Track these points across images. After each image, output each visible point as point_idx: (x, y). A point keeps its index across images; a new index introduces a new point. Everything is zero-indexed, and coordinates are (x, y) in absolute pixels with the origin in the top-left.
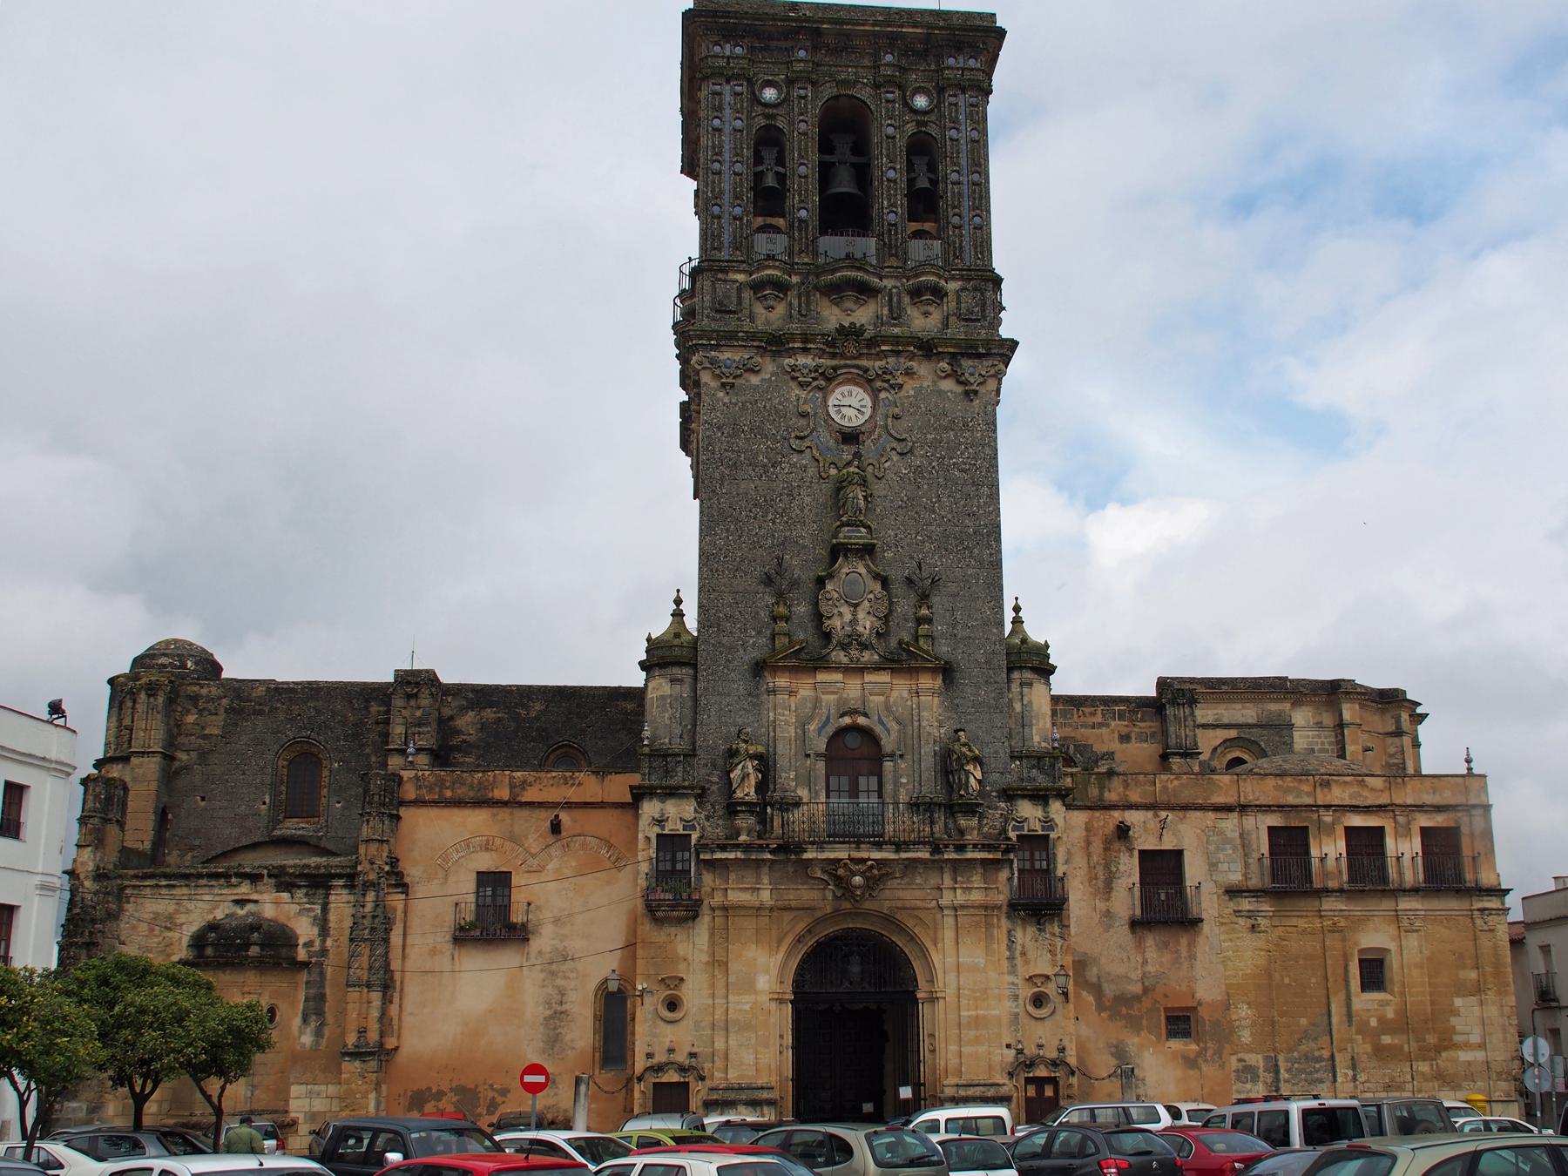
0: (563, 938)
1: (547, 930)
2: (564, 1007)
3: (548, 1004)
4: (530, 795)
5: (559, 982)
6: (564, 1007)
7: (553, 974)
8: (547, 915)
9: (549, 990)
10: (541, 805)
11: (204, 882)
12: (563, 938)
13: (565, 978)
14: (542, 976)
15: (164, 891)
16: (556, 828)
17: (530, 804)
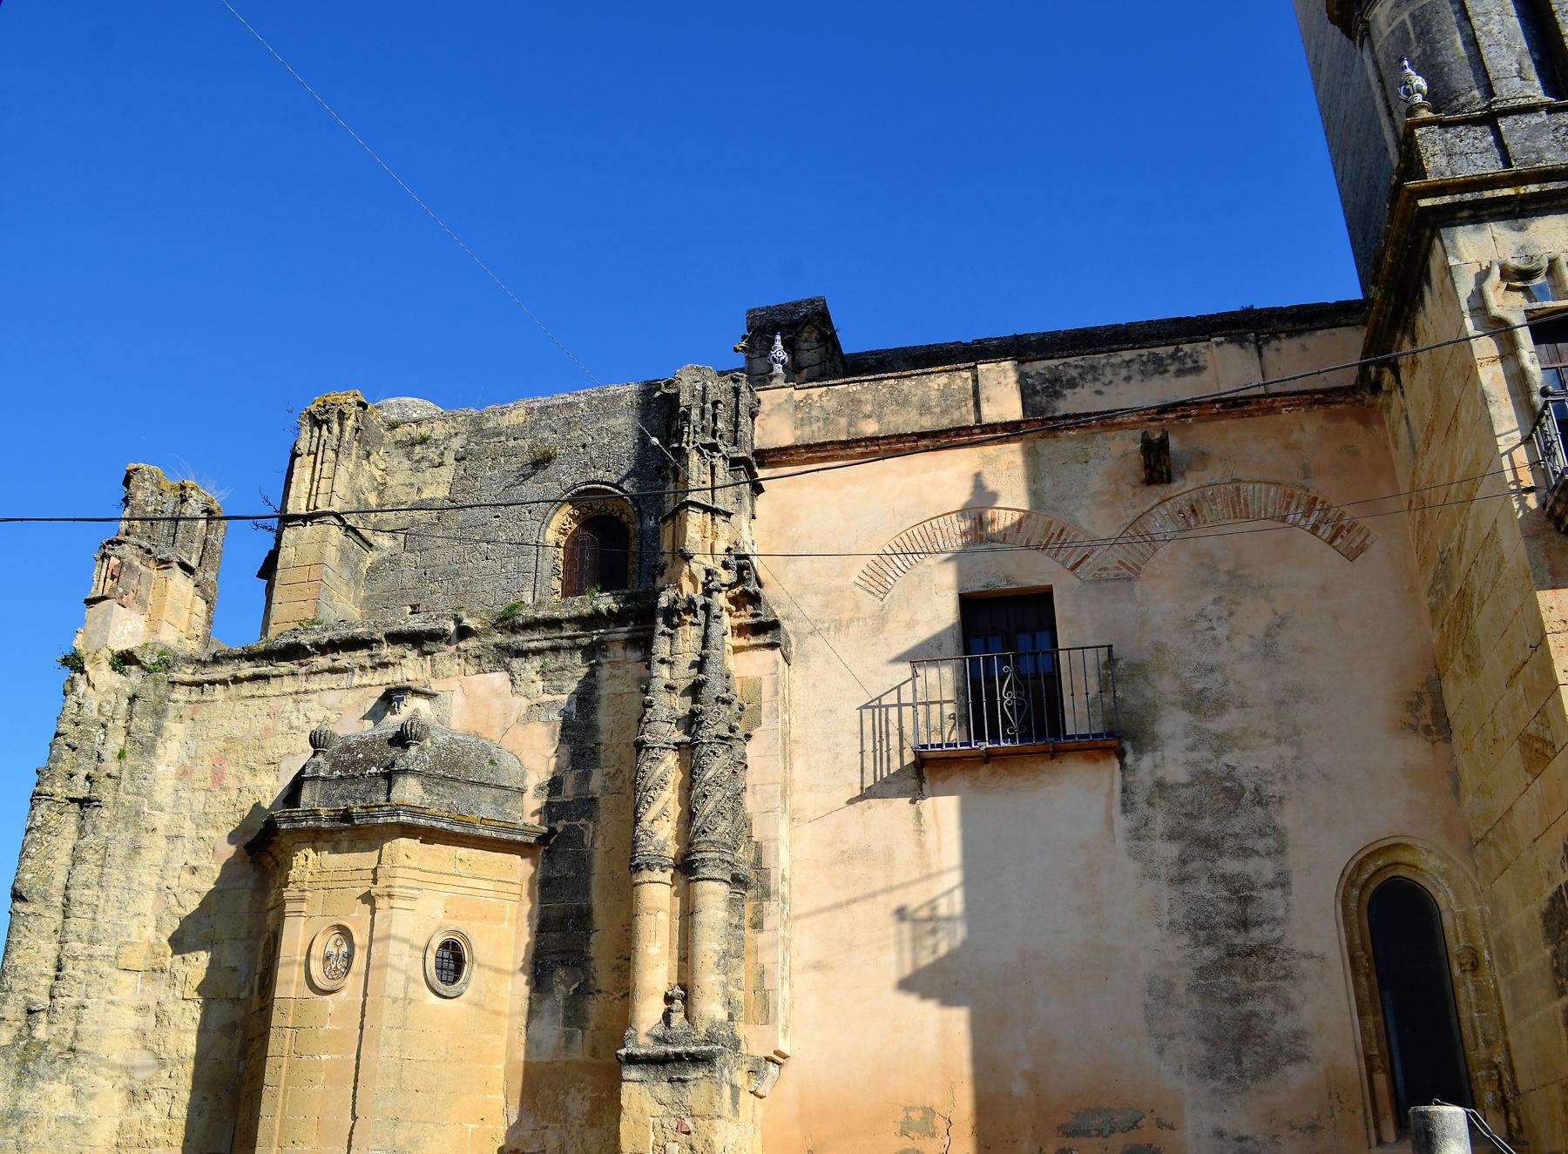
0: (1223, 743)
1: (1172, 724)
2: (1257, 935)
3: (1201, 928)
4: (1075, 401)
5: (1230, 866)
6: (1257, 935)
7: (1209, 844)
8: (1166, 686)
9: (1203, 888)
10: (1107, 420)
11: (322, 662)
12: (1223, 743)
13: (1247, 853)
14: (1173, 850)
15: (247, 688)
16: (1157, 465)
17: (1079, 421)
